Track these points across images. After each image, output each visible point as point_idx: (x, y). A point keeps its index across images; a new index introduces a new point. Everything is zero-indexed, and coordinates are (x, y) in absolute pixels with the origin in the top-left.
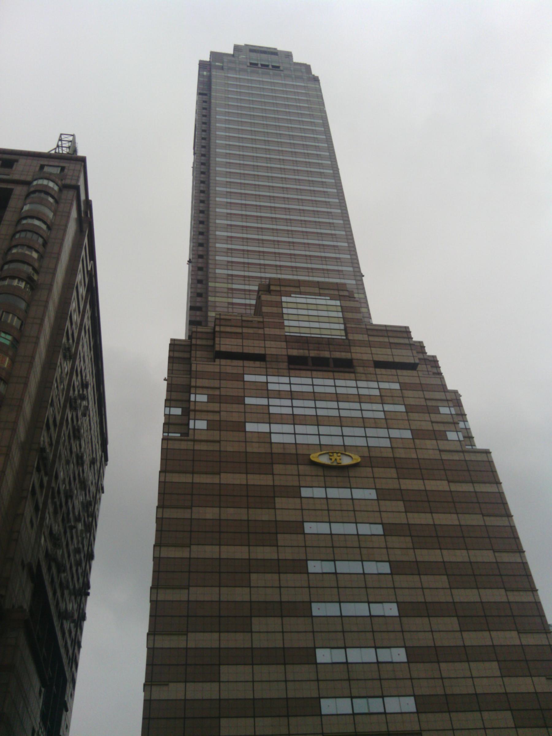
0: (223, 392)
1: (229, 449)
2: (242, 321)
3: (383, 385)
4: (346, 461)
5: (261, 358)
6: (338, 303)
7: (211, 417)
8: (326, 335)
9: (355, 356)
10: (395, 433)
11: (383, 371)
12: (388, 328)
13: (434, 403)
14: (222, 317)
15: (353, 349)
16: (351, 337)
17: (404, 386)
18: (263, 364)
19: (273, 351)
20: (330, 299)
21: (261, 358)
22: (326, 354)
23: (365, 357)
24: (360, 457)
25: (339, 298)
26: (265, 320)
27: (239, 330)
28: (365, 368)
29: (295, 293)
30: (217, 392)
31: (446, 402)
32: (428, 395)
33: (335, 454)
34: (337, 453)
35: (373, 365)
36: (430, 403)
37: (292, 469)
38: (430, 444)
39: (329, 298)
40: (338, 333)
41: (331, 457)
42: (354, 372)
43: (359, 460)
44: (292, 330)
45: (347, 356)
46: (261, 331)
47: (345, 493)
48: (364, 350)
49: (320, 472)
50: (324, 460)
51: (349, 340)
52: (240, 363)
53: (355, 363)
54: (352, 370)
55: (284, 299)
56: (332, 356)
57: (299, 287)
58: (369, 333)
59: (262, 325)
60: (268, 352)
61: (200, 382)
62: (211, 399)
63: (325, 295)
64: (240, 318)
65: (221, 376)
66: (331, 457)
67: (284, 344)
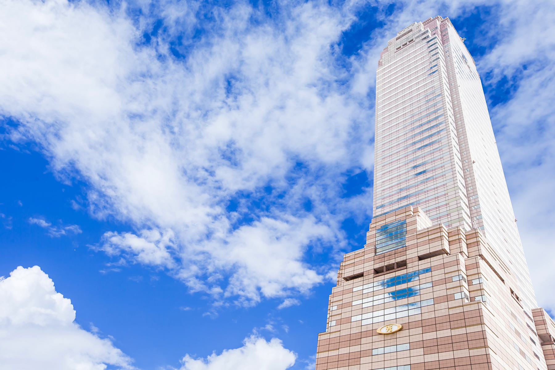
9: (408, 257)
22: (393, 261)
30: (341, 303)
32: (447, 270)
36: (447, 276)
37: (369, 339)
38: (444, 305)
42: (406, 268)
49: (382, 337)
50: (384, 331)
54: (405, 267)
58: (418, 237)
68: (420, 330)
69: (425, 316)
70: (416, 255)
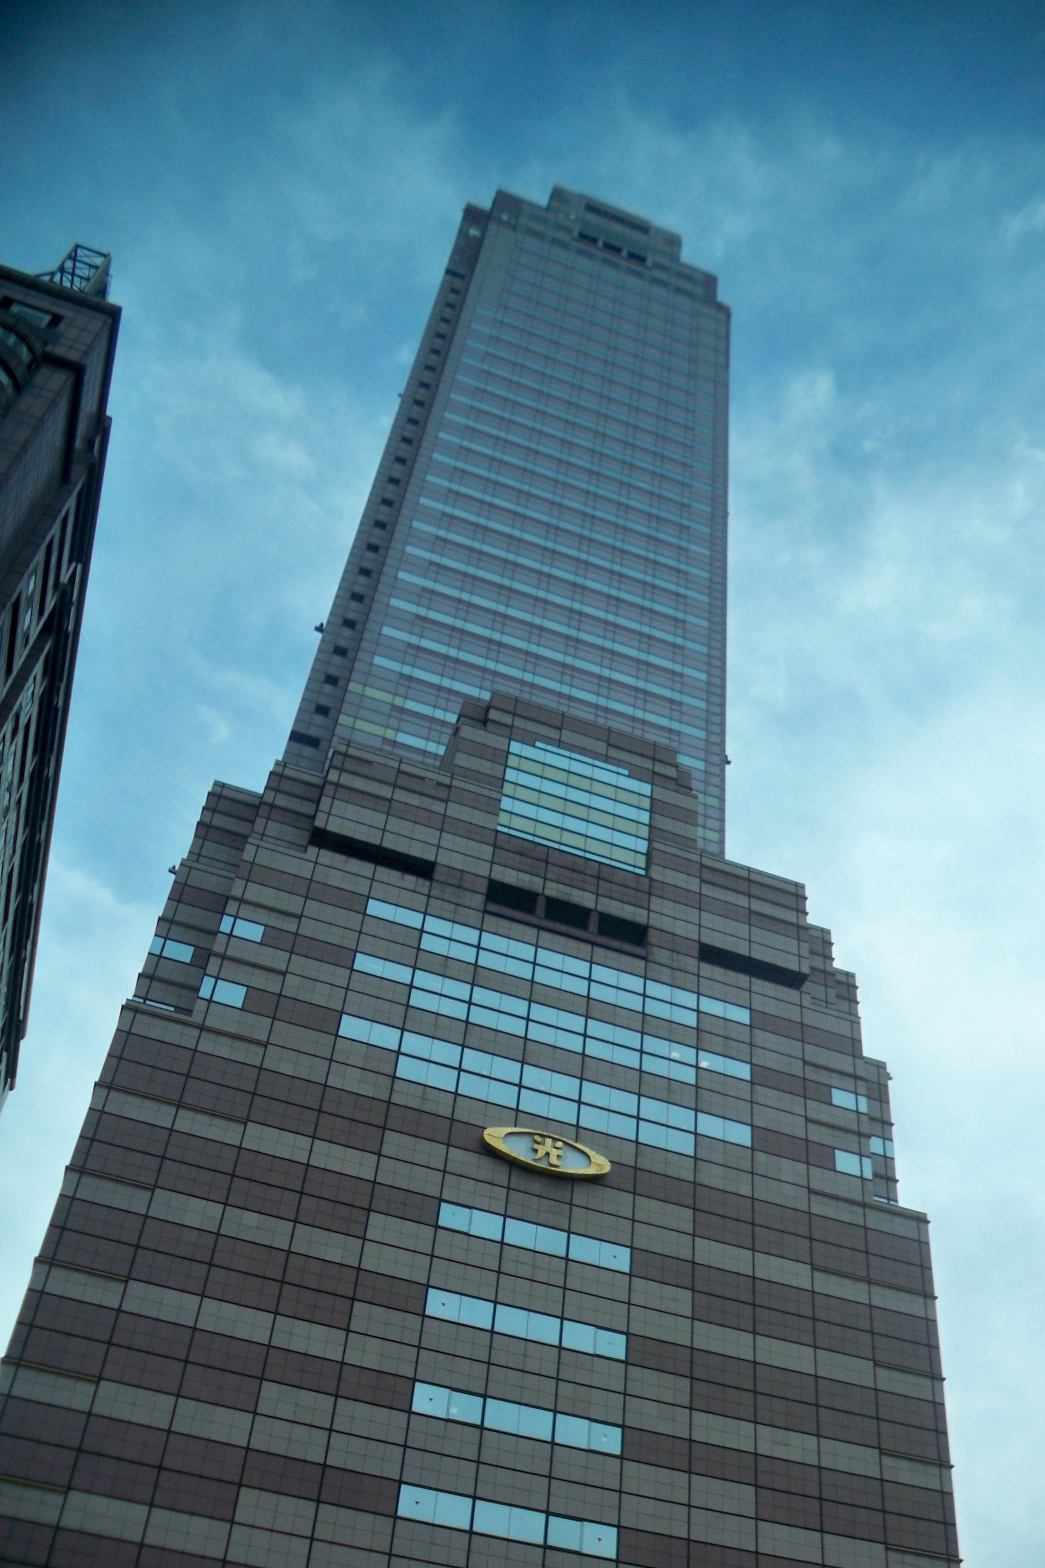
0: (307, 928)
1: (286, 1068)
2: (399, 771)
3: (709, 1006)
4: (573, 1165)
5: (422, 869)
6: (646, 789)
7: (260, 980)
8: (598, 852)
9: (655, 920)
10: (710, 1126)
11: (719, 972)
12: (753, 877)
13: (822, 1077)
14: (352, 751)
15: (656, 903)
16: (656, 873)
17: (760, 1020)
18: (423, 884)
19: (458, 862)
20: (629, 776)
21: (422, 869)
22: (586, 899)
23: (681, 929)
24: (610, 1161)
25: (653, 778)
26: (455, 783)
27: (385, 791)
28: (675, 954)
29: (547, 740)
30: (290, 925)
31: (852, 1081)
32: (814, 1054)
33: (549, 1141)
34: (555, 1140)
35: (696, 954)
36: (811, 1074)
38: (791, 1170)
39: (626, 772)
40: (629, 858)
41: (536, 1146)
43: (607, 1168)
44: (517, 822)
45: (638, 916)
46: (439, 807)
47: (551, 1241)
48: (681, 911)
49: (501, 1174)
50: (519, 1150)
51: (651, 879)
52: (366, 868)
53: (653, 937)
55: (515, 747)
56: (600, 908)
57: (560, 729)
58: (707, 875)
59: (446, 793)
60: (443, 859)
61: (254, 892)
62: (271, 938)
63: (618, 763)
64: (396, 764)
65: (309, 889)
66: (536, 1146)
67: (487, 851)
68: (683, 1218)
69: (712, 1176)
70: (692, 932)
